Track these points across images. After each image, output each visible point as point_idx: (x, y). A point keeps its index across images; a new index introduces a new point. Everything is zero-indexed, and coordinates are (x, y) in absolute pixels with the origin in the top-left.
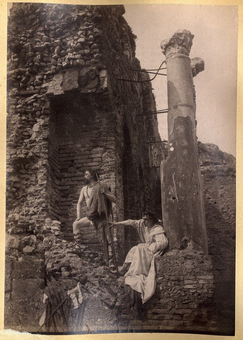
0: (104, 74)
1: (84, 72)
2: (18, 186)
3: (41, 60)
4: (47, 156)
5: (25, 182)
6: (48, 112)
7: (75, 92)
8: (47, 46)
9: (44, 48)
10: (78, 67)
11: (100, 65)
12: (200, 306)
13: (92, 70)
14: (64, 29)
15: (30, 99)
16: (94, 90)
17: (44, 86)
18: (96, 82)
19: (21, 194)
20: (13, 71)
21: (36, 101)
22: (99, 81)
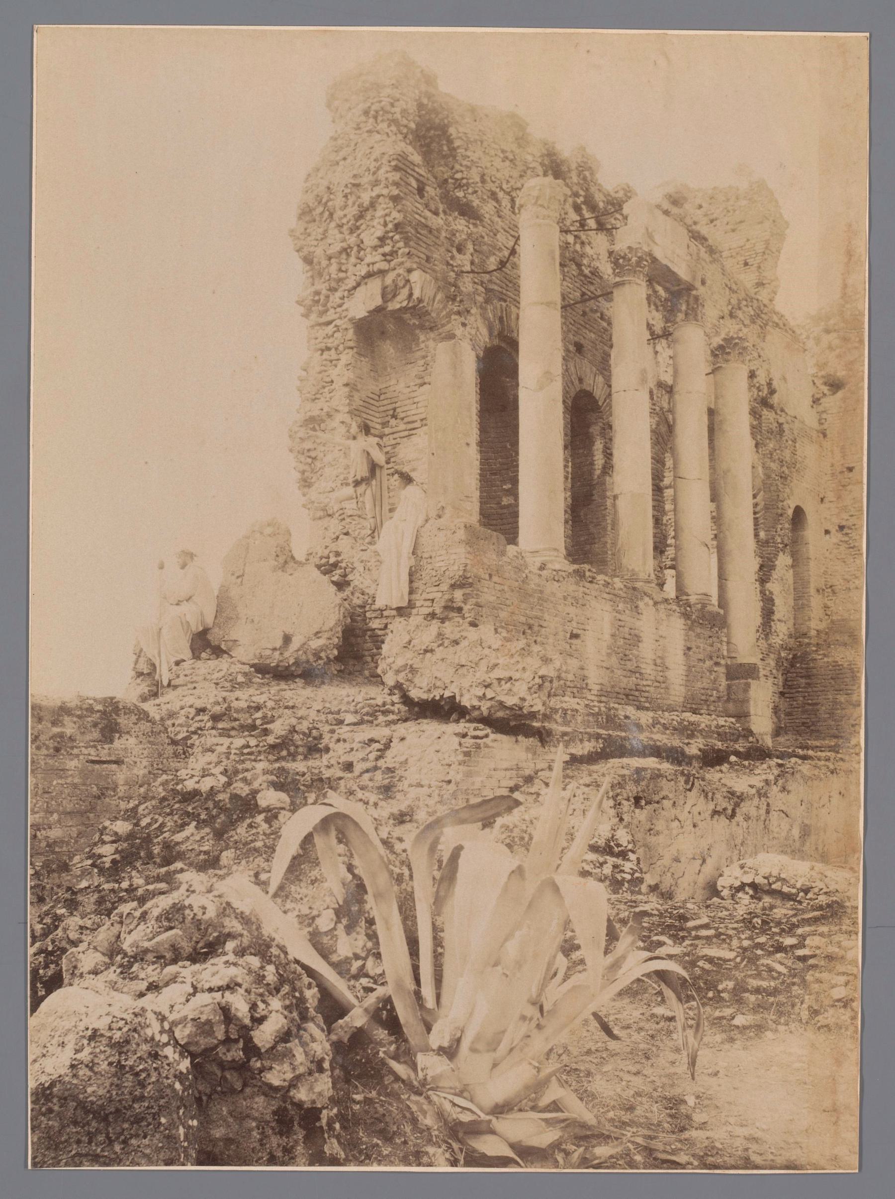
0: (415, 276)
1: (389, 279)
2: (313, 454)
3: (340, 270)
4: (347, 409)
5: (322, 448)
6: (351, 344)
7: (379, 310)
8: (344, 250)
9: (340, 253)
10: (382, 273)
11: (408, 265)
12: (453, 586)
13: (399, 275)
14: (357, 221)
15: (330, 329)
16: (405, 304)
17: (344, 307)
18: (405, 292)
19: (318, 464)
20: (309, 291)
21: (338, 331)
22: (411, 289)
